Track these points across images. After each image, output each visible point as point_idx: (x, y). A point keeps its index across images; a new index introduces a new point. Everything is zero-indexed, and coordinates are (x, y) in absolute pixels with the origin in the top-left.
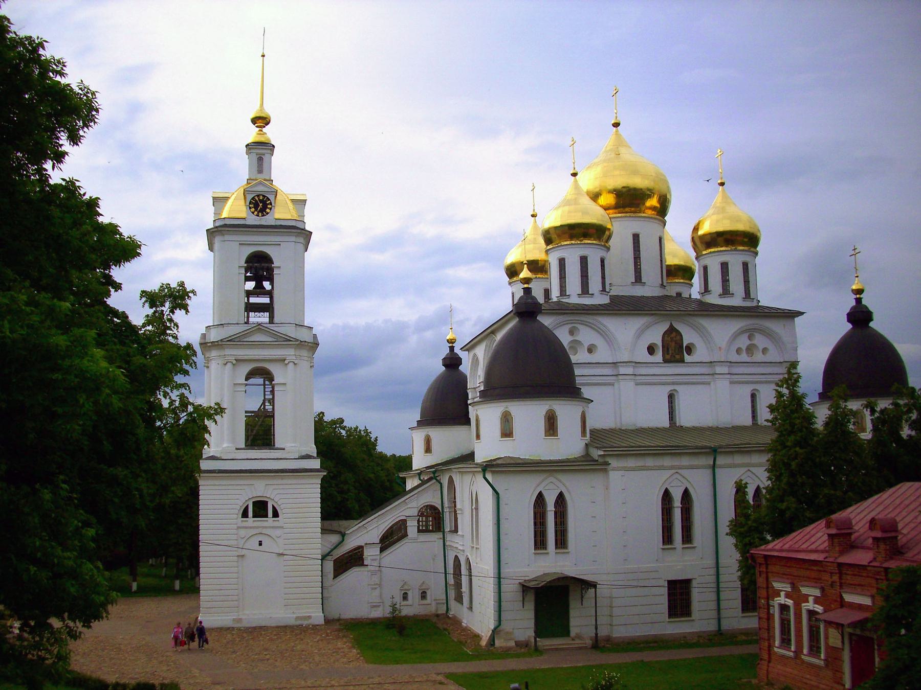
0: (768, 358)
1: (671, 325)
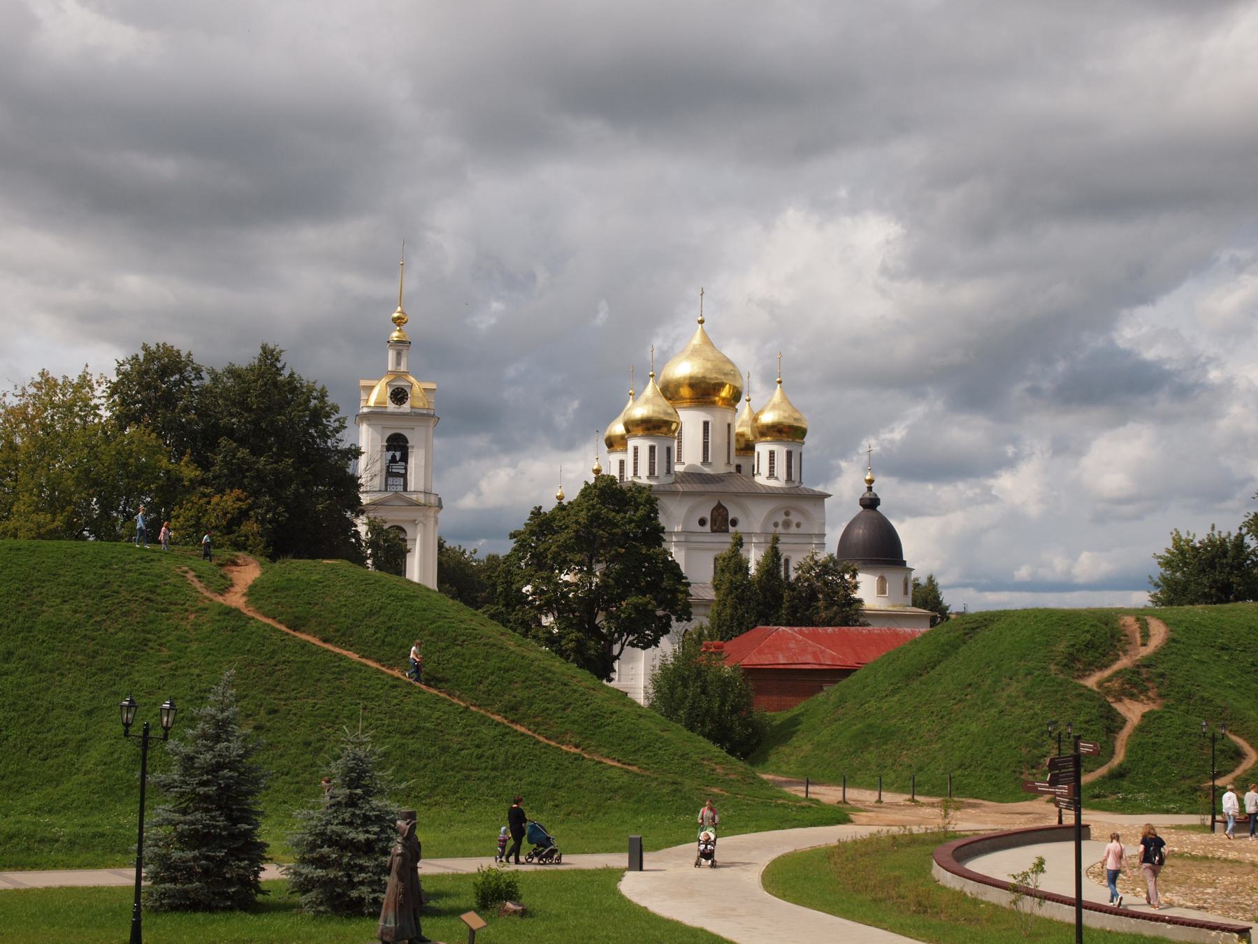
0: (801, 531)
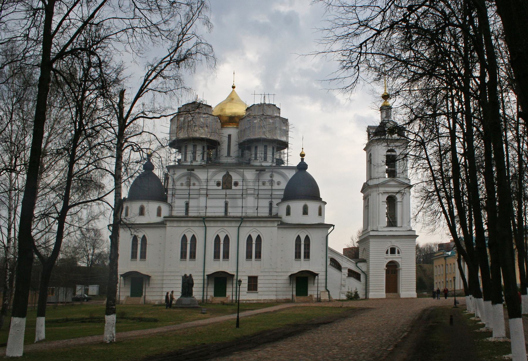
1: (228, 173)
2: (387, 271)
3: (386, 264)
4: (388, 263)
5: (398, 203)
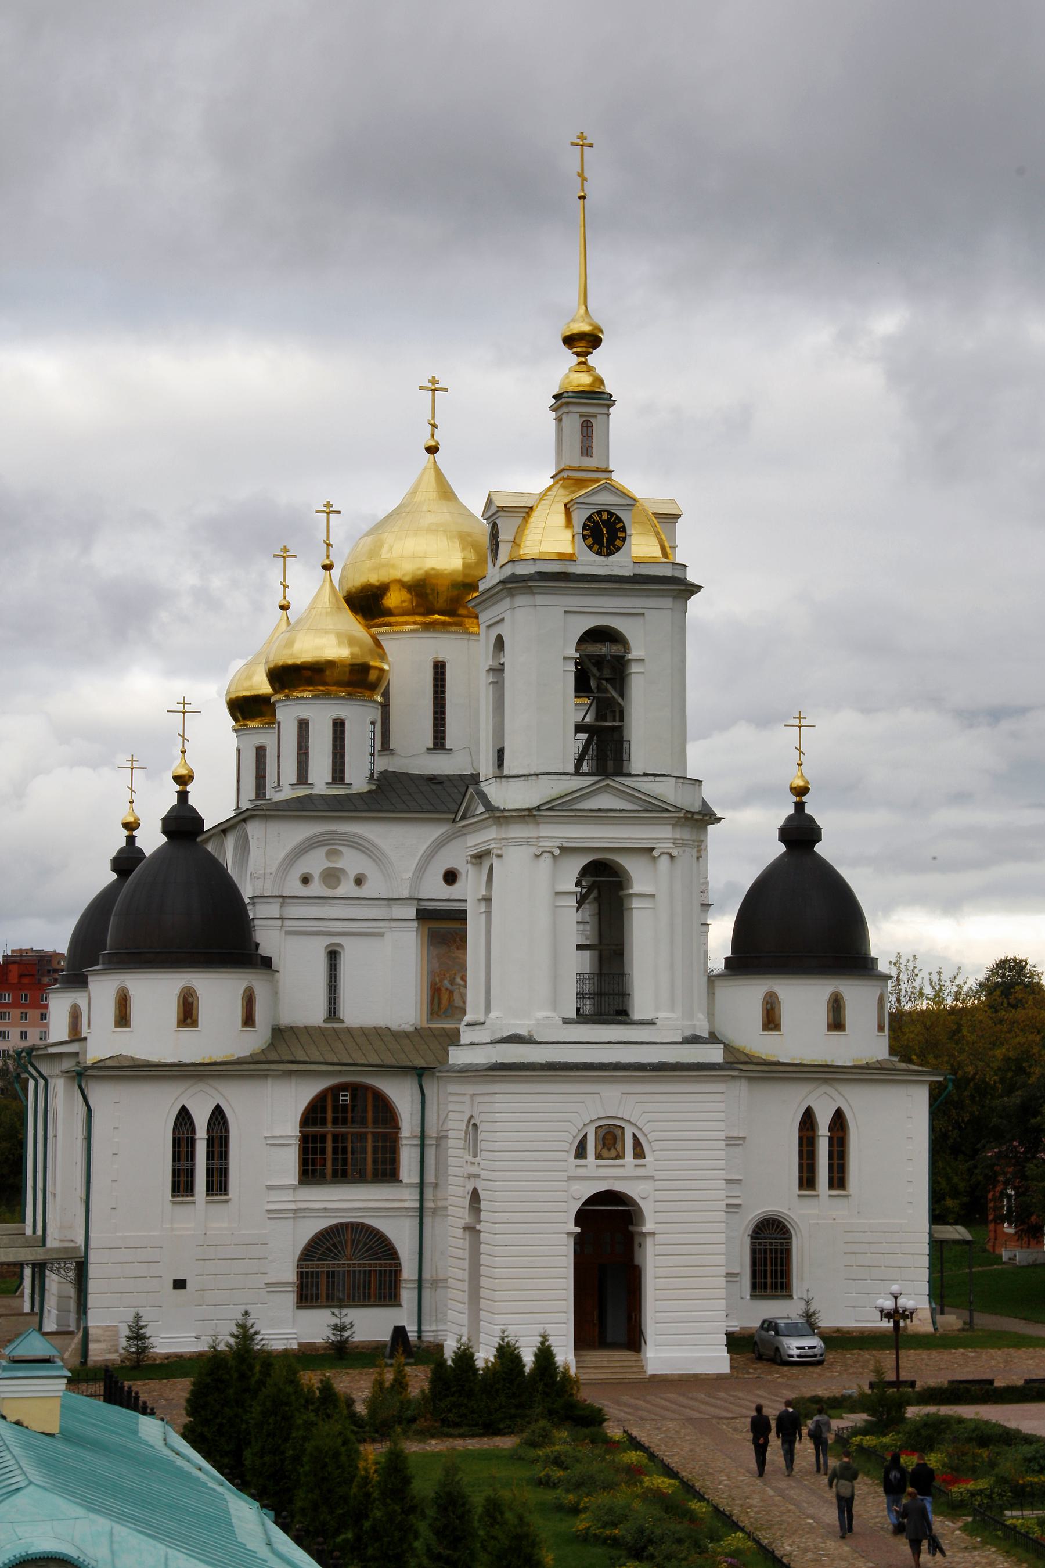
2: (579, 1242)
3: (577, 1206)
4: (587, 1202)
5: (636, 903)
